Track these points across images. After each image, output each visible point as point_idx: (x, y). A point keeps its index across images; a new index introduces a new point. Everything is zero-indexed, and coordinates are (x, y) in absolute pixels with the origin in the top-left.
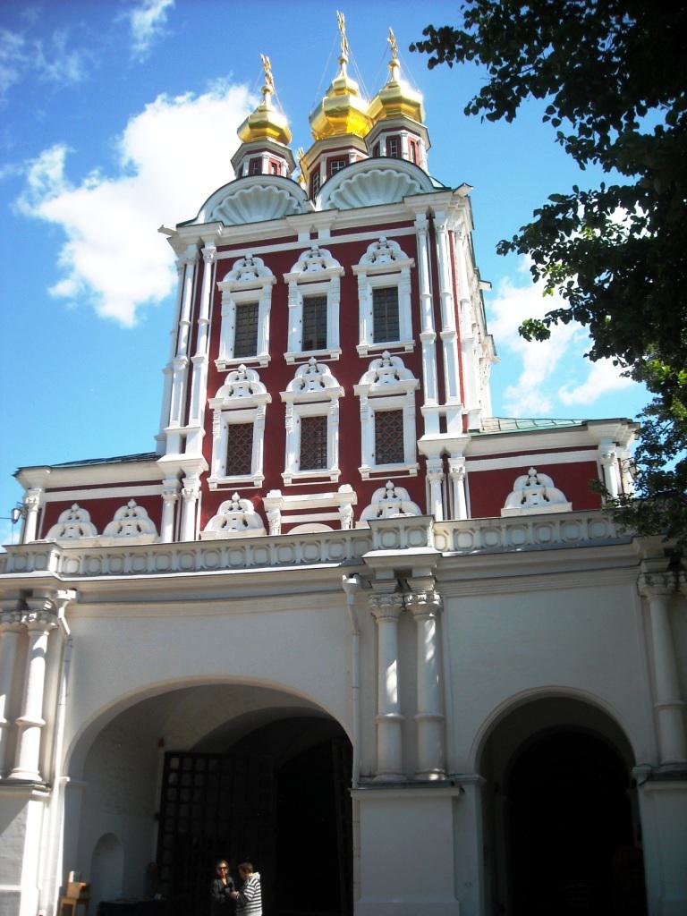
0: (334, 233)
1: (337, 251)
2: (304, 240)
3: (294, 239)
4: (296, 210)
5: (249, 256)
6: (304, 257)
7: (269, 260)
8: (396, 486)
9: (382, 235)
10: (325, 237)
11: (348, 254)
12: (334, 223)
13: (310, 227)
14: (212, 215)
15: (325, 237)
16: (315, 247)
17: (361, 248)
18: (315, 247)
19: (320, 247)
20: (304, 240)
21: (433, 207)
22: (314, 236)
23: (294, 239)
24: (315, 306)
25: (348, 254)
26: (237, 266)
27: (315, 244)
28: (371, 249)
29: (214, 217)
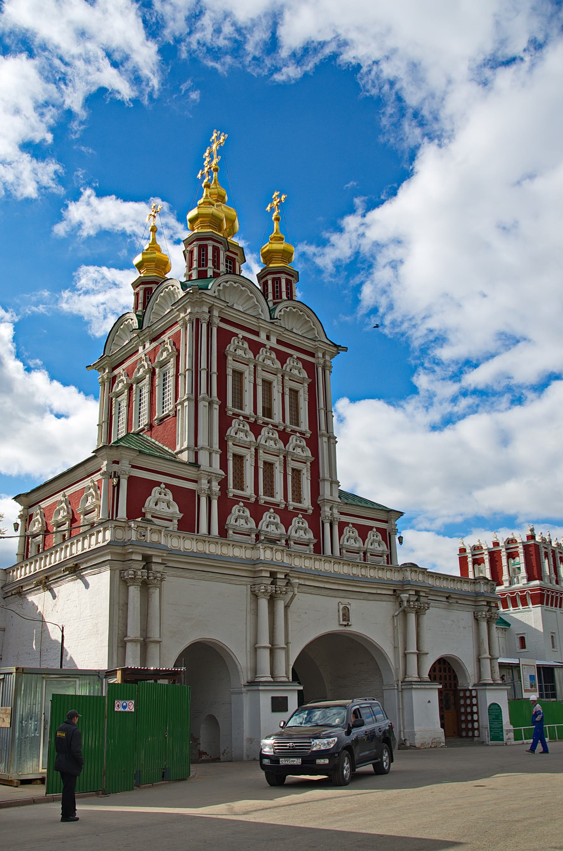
0: (279, 342)
3: (257, 334)
4: (260, 314)
8: (303, 518)
10: (273, 342)
12: (280, 334)
13: (267, 331)
14: (215, 292)
15: (273, 342)
18: (268, 347)
19: (272, 349)
20: (262, 338)
21: (327, 352)
22: (268, 338)
23: (257, 334)
29: (216, 294)
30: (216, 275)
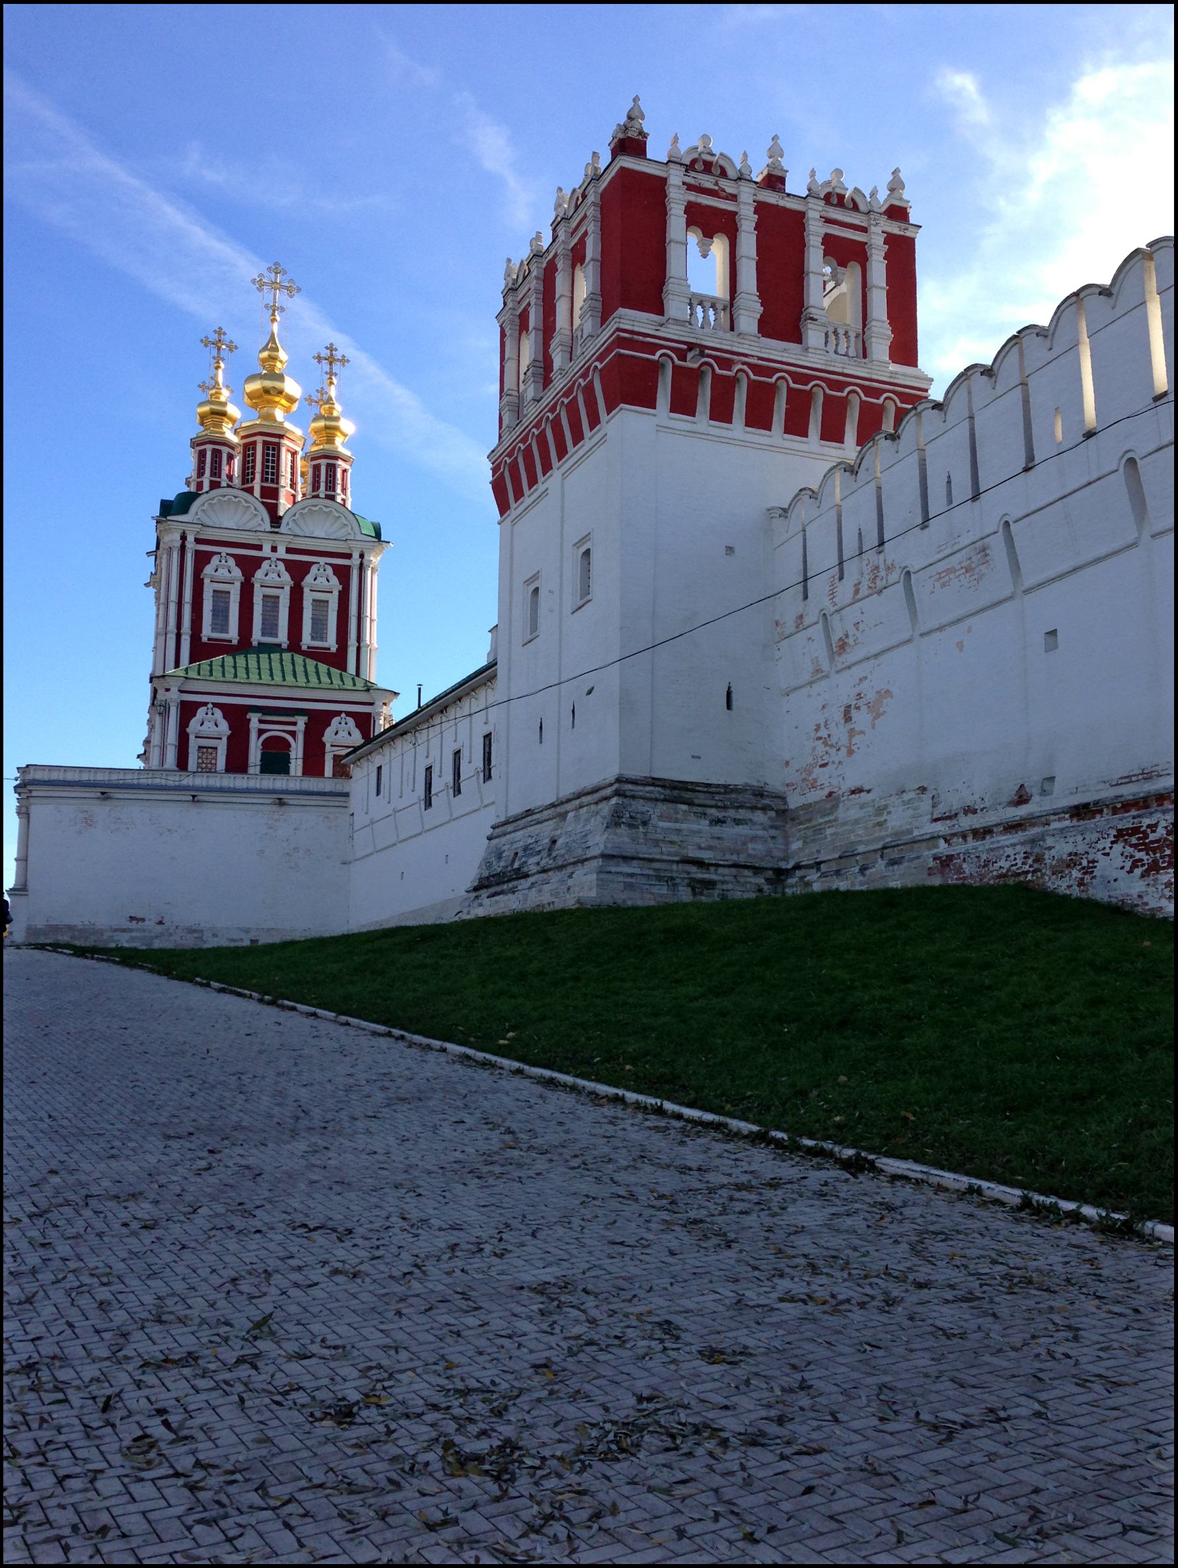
1: (289, 565)
2: (266, 551)
5: (224, 555)
6: (265, 565)
7: (241, 561)
9: (322, 560)
11: (298, 571)
15: (281, 553)
16: (274, 559)
17: (304, 568)
18: (274, 559)
20: (266, 551)
22: (274, 549)
23: (259, 548)
24: (271, 603)
25: (298, 571)
26: (215, 560)
27: (274, 556)
28: (314, 569)
30: (215, 485)
